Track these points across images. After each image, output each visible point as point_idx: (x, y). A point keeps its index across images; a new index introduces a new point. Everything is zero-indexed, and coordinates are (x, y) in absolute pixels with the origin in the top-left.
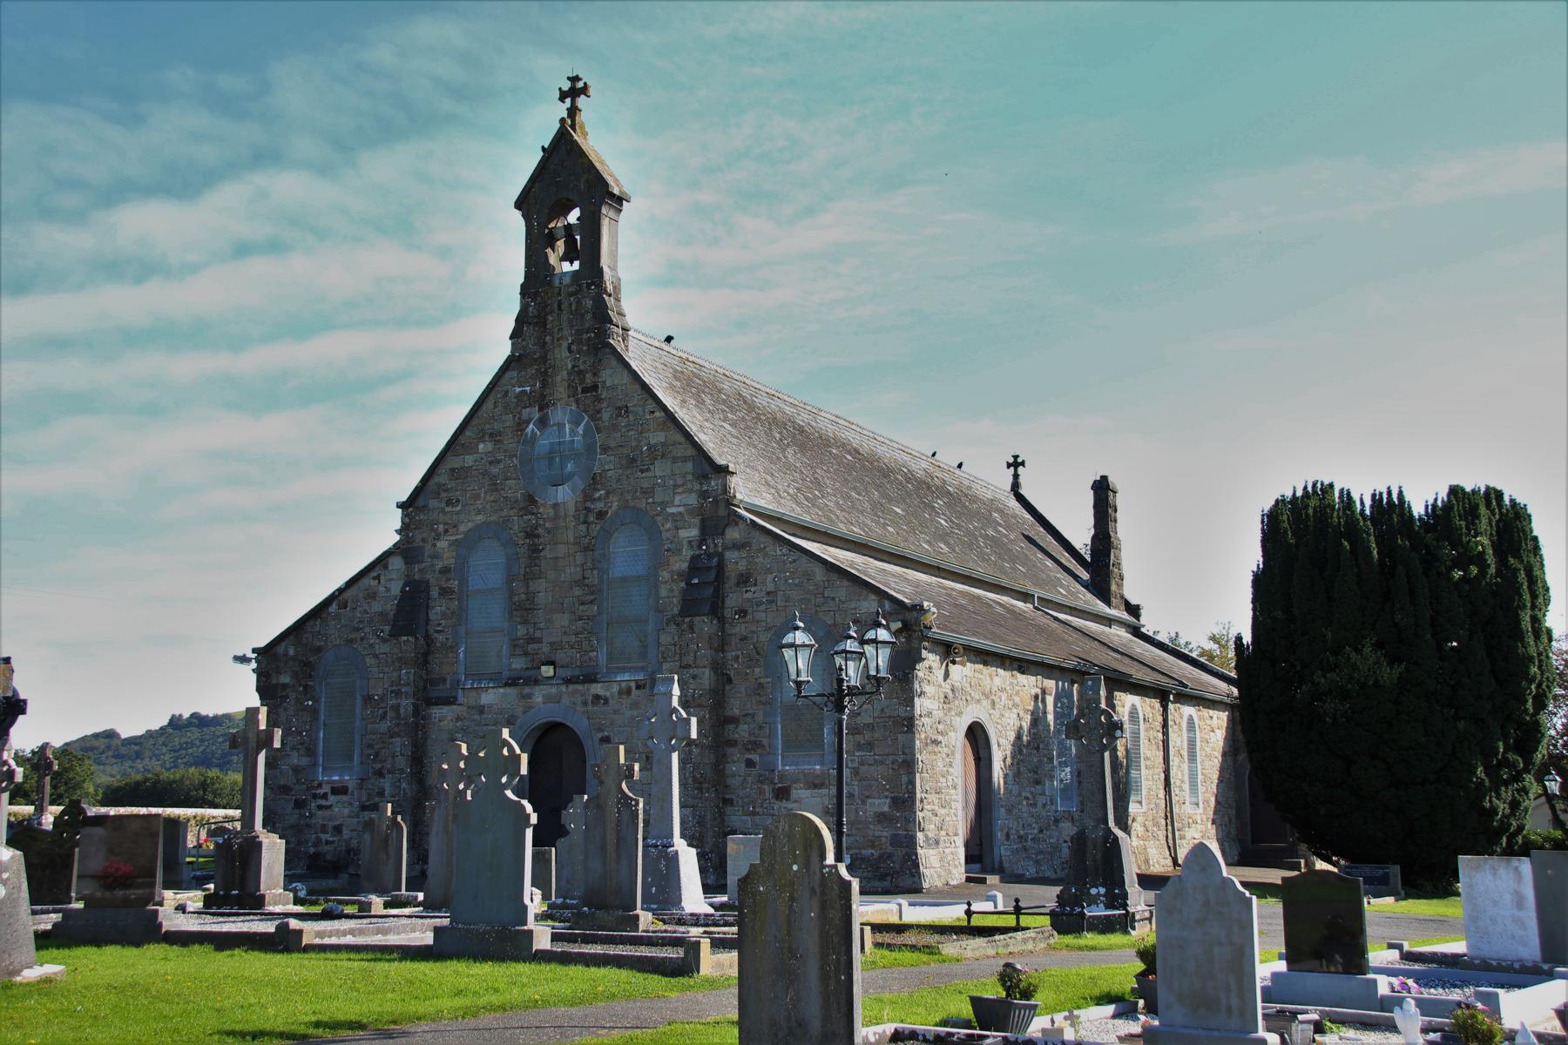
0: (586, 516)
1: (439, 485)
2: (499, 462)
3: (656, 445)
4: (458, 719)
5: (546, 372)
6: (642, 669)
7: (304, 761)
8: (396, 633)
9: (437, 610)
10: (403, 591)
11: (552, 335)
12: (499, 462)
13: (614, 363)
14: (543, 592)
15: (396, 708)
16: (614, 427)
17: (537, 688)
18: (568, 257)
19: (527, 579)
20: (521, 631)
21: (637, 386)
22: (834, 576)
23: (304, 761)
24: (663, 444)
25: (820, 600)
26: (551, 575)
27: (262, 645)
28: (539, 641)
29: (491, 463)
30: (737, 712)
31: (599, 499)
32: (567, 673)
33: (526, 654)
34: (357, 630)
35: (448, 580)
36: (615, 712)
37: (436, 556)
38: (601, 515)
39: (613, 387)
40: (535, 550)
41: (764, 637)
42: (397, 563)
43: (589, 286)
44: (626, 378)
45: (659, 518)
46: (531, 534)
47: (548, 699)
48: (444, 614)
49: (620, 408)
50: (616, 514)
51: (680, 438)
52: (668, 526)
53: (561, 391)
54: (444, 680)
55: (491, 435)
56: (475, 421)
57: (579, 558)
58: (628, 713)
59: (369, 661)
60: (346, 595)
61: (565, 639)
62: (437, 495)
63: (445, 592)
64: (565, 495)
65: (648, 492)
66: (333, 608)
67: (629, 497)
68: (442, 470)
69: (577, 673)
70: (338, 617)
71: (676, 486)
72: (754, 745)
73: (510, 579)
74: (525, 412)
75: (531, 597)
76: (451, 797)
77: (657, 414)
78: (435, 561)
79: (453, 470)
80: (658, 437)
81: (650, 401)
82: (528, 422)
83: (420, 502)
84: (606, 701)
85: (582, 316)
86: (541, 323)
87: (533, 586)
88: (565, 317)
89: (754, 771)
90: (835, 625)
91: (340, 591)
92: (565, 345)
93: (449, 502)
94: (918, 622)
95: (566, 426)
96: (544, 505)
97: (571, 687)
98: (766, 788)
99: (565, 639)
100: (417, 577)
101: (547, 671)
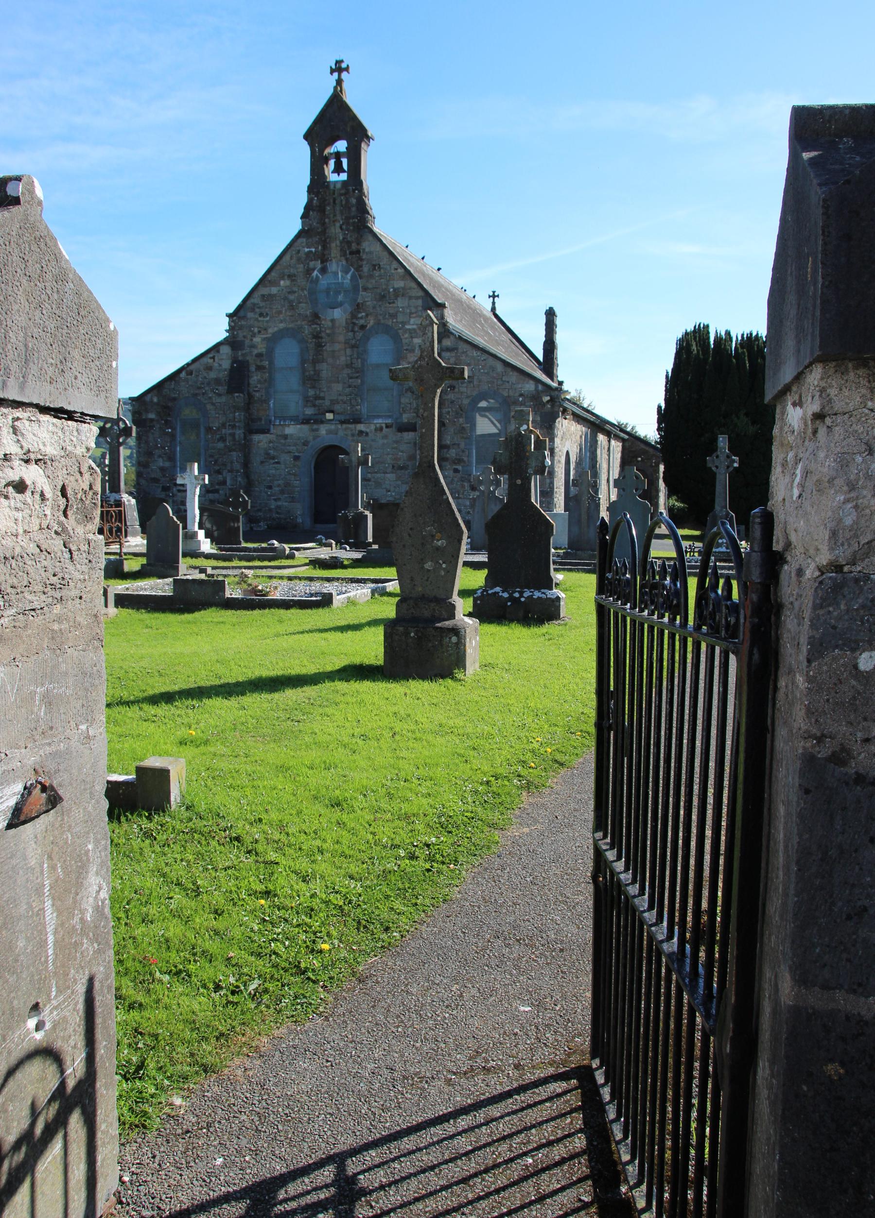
0: (353, 328)
1: (254, 304)
2: (294, 292)
3: (398, 288)
4: (270, 442)
5: (325, 241)
6: (390, 417)
7: (167, 464)
8: (231, 391)
9: (255, 378)
10: (232, 366)
11: (329, 218)
12: (294, 292)
13: (371, 238)
14: (325, 370)
15: (233, 435)
16: (371, 276)
17: (322, 426)
18: (338, 169)
19: (315, 362)
20: (311, 392)
21: (386, 253)
22: (509, 370)
23: (167, 464)
24: (404, 288)
25: (500, 382)
26: (330, 360)
27: (136, 395)
28: (323, 398)
29: (289, 293)
30: (448, 442)
31: (361, 318)
32: (342, 418)
33: (314, 406)
34: (199, 388)
35: (261, 361)
36: (373, 440)
37: (253, 346)
38: (363, 327)
39: (371, 253)
40: (319, 346)
41: (466, 402)
42: (226, 350)
43: (354, 191)
44: (378, 248)
45: (400, 332)
46: (317, 336)
47: (329, 432)
48: (259, 382)
49: (374, 266)
50: (372, 327)
51: (413, 285)
52: (407, 335)
53: (335, 250)
54: (260, 419)
55: (289, 276)
56: (278, 267)
57: (349, 351)
58: (381, 442)
59: (209, 407)
60: (192, 367)
61: (340, 398)
62: (253, 310)
63: (259, 368)
64: (338, 314)
65: (393, 316)
66: (183, 375)
67: (381, 318)
68: (256, 295)
69: (347, 417)
70: (186, 380)
71: (411, 313)
72: (459, 461)
73: (303, 362)
74: (312, 264)
75: (317, 373)
76: (486, 495)
77: (399, 270)
78: (253, 349)
79: (263, 296)
80: (400, 284)
81: (395, 262)
82: (314, 270)
83: (241, 313)
84: (367, 434)
85: (350, 208)
86: (321, 209)
87: (318, 367)
88: (338, 208)
89: (459, 475)
90: (509, 396)
91: (188, 365)
92: (338, 225)
93: (261, 315)
94: (558, 397)
95: (339, 274)
96: (325, 320)
97: (344, 426)
98: (466, 484)
99: (340, 398)
100: (240, 358)
101: (329, 416)
